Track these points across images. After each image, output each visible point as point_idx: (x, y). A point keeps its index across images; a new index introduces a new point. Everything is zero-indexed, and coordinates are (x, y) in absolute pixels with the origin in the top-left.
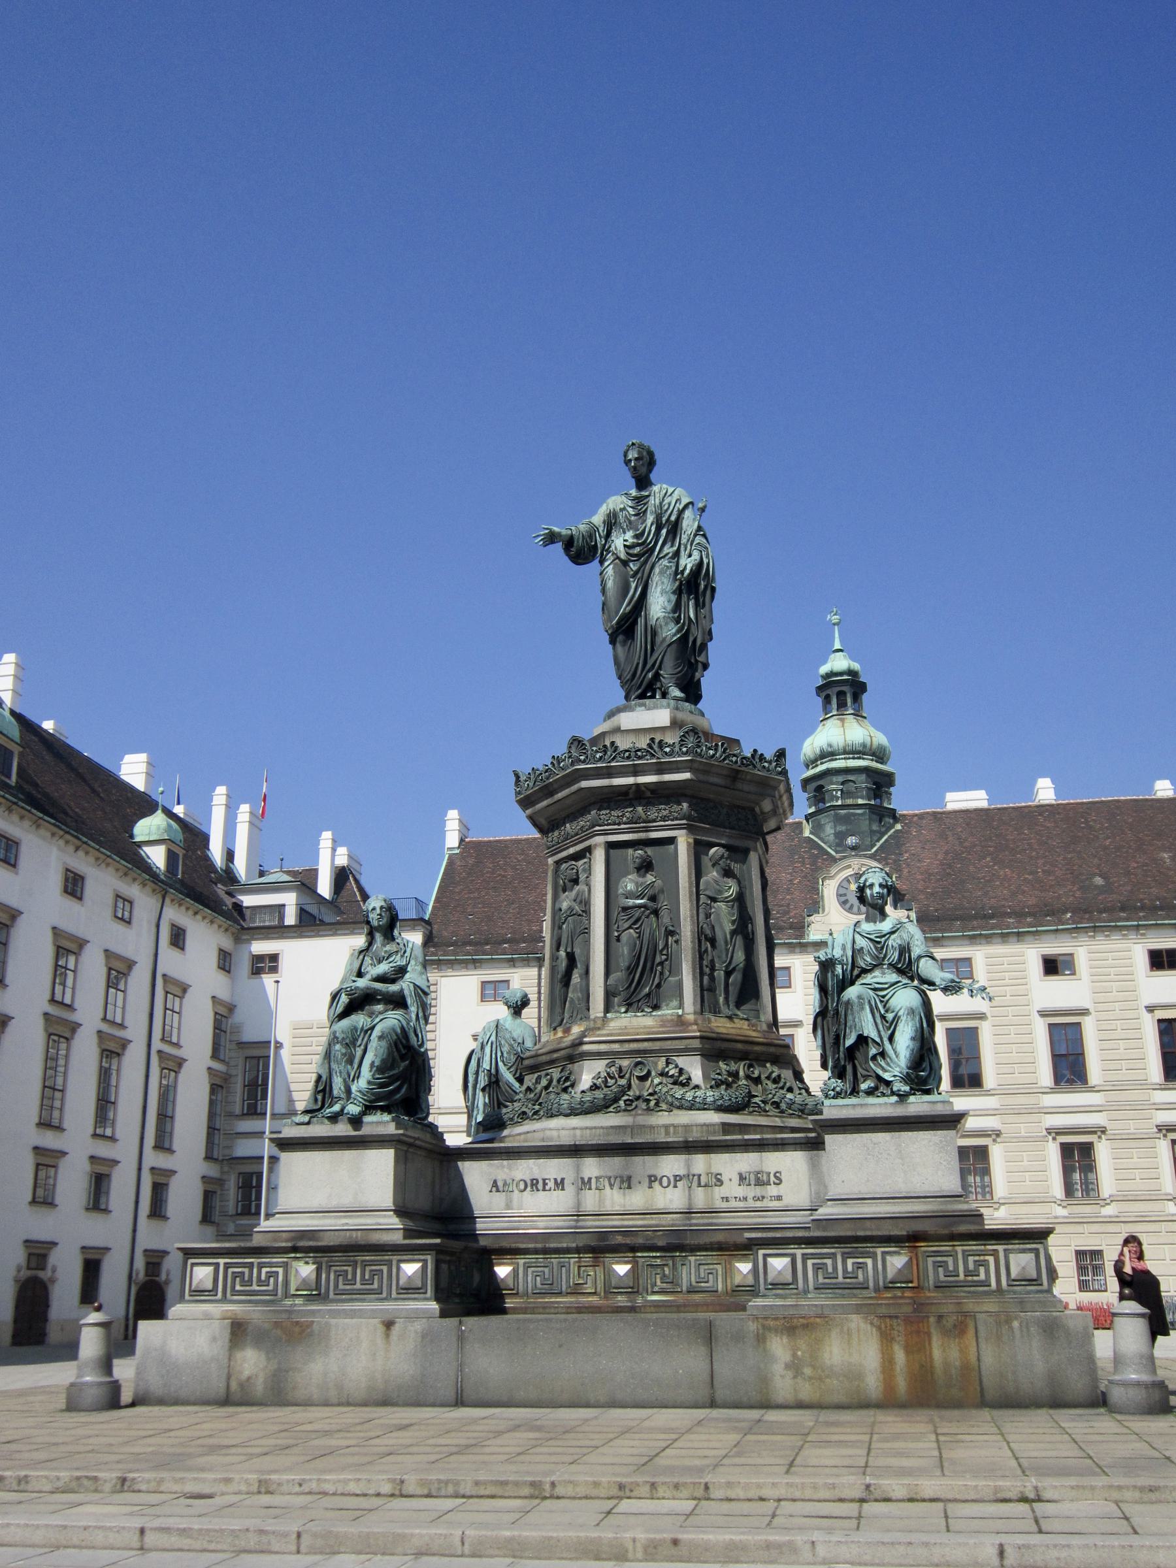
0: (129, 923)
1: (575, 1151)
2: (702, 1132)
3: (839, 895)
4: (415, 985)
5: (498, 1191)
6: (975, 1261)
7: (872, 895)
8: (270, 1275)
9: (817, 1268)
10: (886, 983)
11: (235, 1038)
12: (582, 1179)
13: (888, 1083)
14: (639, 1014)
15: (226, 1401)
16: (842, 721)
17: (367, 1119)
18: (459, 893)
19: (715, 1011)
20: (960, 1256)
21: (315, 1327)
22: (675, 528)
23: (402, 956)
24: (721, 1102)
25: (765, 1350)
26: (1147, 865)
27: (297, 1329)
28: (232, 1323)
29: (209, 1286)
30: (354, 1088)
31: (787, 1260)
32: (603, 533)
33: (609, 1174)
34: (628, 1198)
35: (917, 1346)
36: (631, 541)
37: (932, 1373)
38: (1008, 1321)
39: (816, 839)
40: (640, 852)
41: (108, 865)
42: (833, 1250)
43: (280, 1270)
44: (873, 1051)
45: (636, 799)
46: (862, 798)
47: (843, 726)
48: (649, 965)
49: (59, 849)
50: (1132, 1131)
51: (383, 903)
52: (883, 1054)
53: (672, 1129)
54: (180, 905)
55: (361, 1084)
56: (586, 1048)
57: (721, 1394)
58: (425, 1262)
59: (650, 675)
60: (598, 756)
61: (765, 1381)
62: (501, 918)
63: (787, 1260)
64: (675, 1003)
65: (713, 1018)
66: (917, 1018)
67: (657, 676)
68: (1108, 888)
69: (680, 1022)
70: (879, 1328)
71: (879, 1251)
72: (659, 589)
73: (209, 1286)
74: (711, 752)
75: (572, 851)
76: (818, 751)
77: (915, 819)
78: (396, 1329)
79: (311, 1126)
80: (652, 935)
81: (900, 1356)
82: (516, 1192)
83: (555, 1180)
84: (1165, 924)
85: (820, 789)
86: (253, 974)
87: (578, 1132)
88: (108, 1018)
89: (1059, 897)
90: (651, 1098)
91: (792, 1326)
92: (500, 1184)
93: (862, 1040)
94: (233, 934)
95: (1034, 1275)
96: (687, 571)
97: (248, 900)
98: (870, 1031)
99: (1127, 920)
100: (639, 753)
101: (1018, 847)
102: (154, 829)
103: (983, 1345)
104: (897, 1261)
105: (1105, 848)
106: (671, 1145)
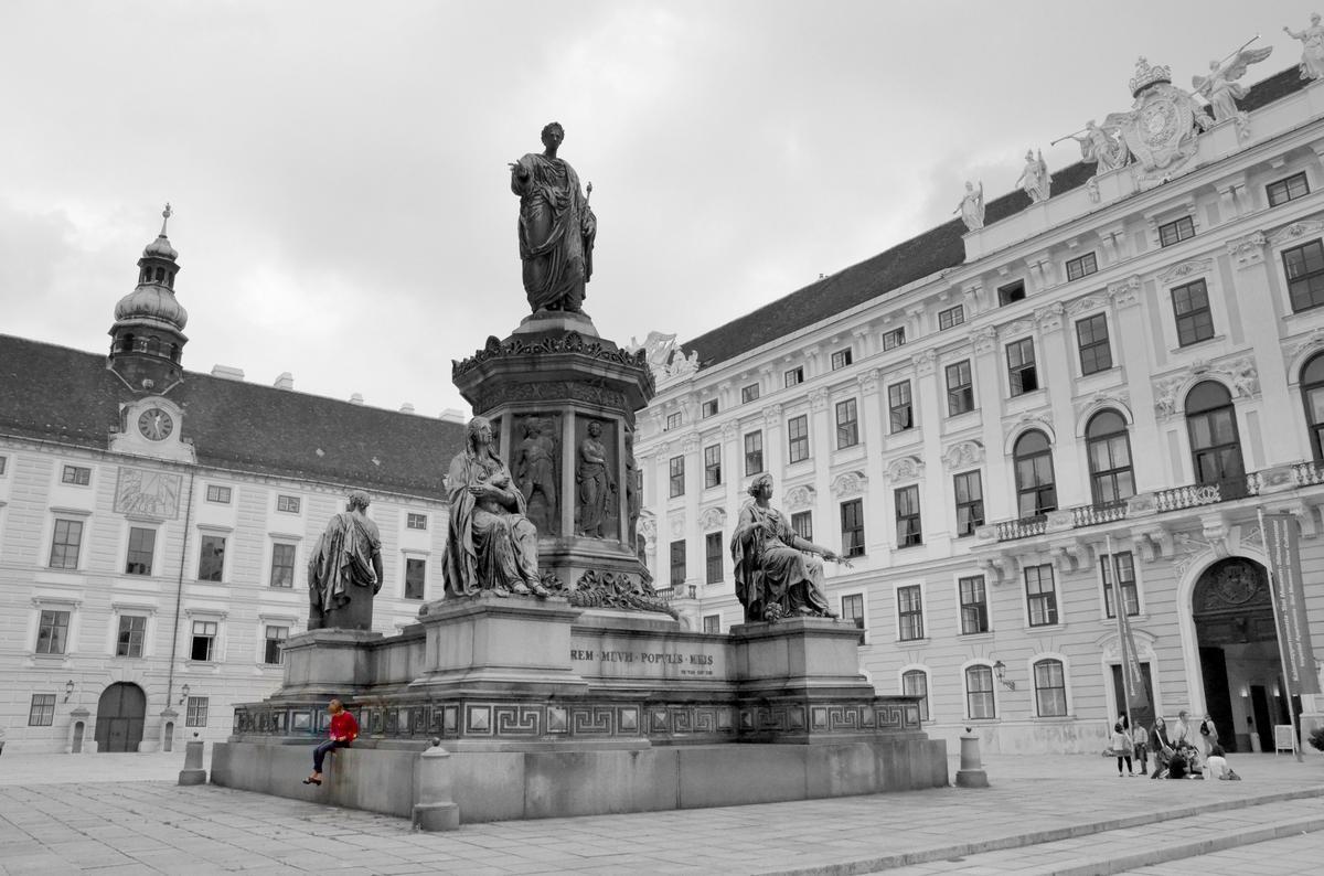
1: (602, 633)
3: (140, 422)
13: (820, 610)
15: (524, 817)
16: (158, 290)
21: (586, 757)
27: (573, 759)
29: (487, 726)
35: (888, 761)
43: (538, 713)
44: (811, 590)
52: (815, 591)
55: (532, 570)
56: (572, 558)
59: (562, 294)
61: (828, 781)
64: (614, 535)
75: (536, 409)
76: (135, 308)
87: (599, 620)
89: (296, 457)
93: (805, 582)
99: (338, 482)
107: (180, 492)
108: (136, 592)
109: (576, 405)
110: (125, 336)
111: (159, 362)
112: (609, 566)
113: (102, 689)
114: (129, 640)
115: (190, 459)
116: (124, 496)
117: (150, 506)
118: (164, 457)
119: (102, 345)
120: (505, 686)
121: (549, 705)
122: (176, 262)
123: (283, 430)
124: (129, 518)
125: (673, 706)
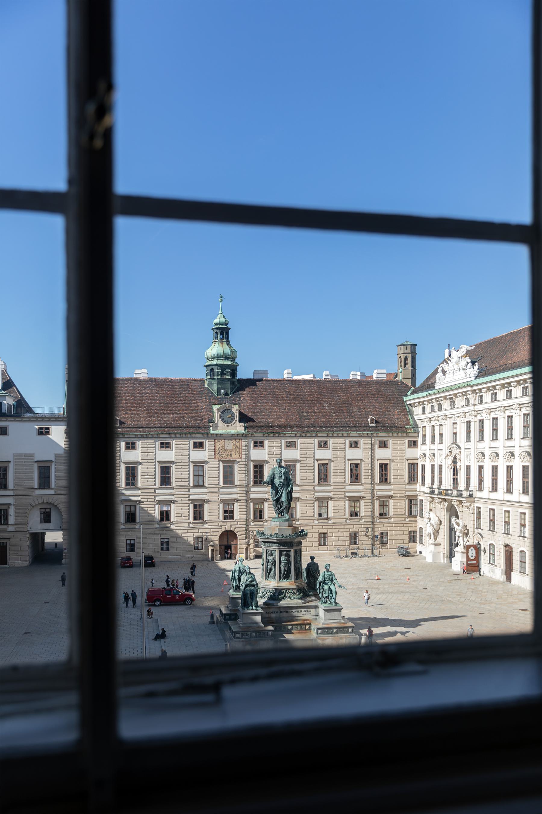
16: (222, 344)
26: (320, 408)
39: (210, 389)
44: (330, 598)
46: (228, 376)
47: (222, 347)
50: (307, 498)
67: (283, 511)
68: (308, 417)
76: (213, 356)
77: (244, 382)
84: (324, 433)
85: (212, 370)
98: (330, 595)
99: (313, 431)
101: (279, 398)
105: (307, 401)
107: (241, 446)
108: (228, 493)
110: (211, 370)
111: (226, 380)
113: (219, 534)
114: (229, 515)
115: (243, 431)
116: (218, 451)
117: (229, 454)
118: (233, 431)
119: (202, 374)
122: (229, 326)
123: (287, 404)
124: (222, 461)
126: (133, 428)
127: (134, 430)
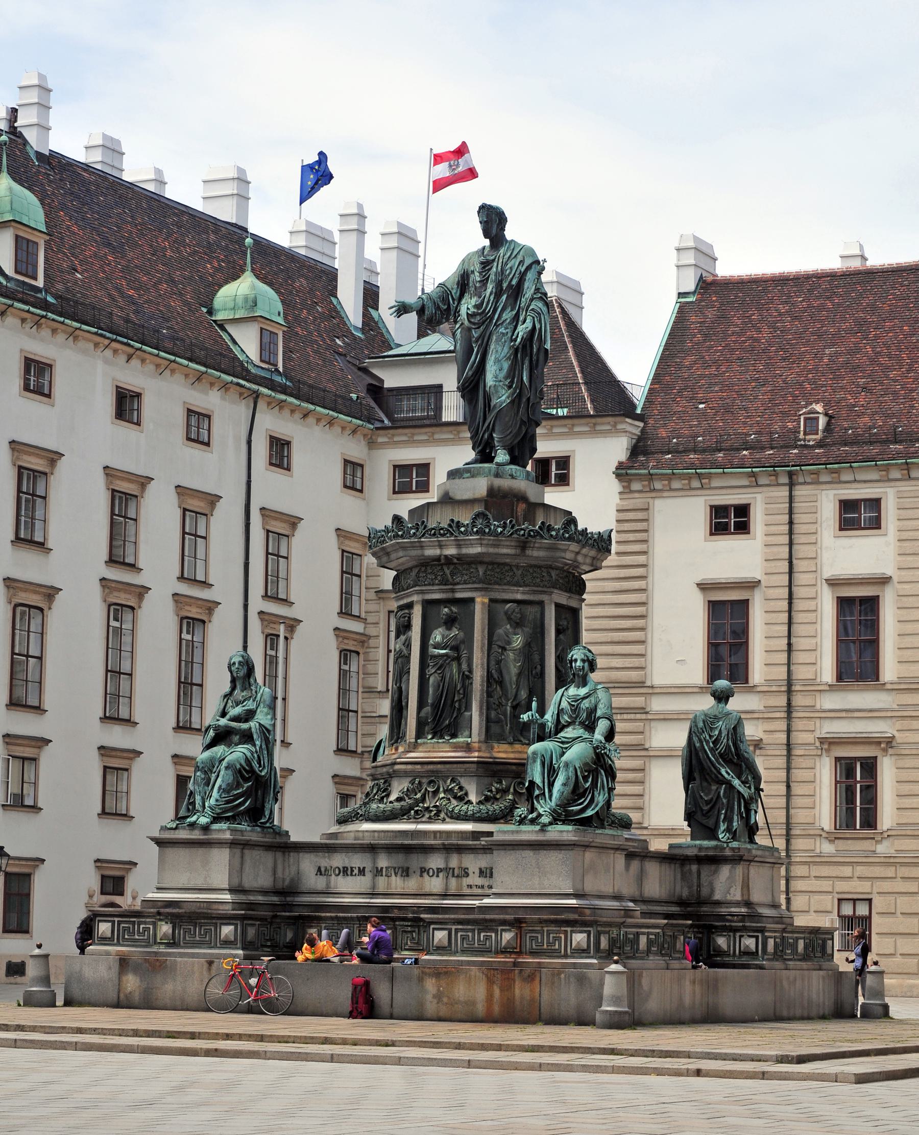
0: (208, 444)
1: (372, 849)
2: (458, 837)
4: (260, 724)
5: (321, 874)
6: (553, 937)
7: (575, 667)
8: (145, 929)
9: (463, 939)
10: (570, 738)
11: (372, 584)
12: (377, 868)
14: (440, 741)
15: (118, 1005)
17: (215, 826)
18: (690, 368)
19: (501, 738)
20: (545, 934)
22: (517, 291)
23: (254, 701)
24: (478, 815)
25: (423, 986)
27: (158, 964)
28: (120, 959)
29: (109, 935)
30: (207, 804)
31: (445, 933)
32: (456, 296)
33: (395, 865)
34: (406, 883)
35: (507, 988)
36: (472, 310)
37: (514, 1003)
38: (559, 974)
40: (446, 610)
41: (173, 371)
42: (473, 927)
43: (151, 927)
45: (446, 564)
48: (449, 702)
49: (106, 361)
51: (241, 659)
52: (544, 793)
53: (438, 834)
54: (281, 408)
56: (397, 767)
57: (396, 1011)
58: (236, 925)
59: (486, 436)
60: (412, 531)
61: (421, 1004)
62: (746, 409)
63: (445, 933)
64: (467, 733)
65: (496, 745)
66: (571, 769)
67: (491, 437)
69: (468, 748)
70: (487, 976)
71: (500, 928)
72: (493, 358)
73: (109, 935)
74: (499, 530)
78: (214, 966)
79: (177, 831)
80: (451, 677)
81: (497, 992)
82: (333, 876)
83: (359, 868)
86: (394, 492)
87: (376, 834)
88: (186, 575)
90: (434, 809)
91: (440, 972)
92: (323, 870)
93: (532, 783)
94: (365, 436)
95: (585, 946)
96: (519, 340)
97: (392, 379)
100: (442, 532)
102: (240, 301)
103: (543, 988)
104: (507, 936)
106: (435, 847)
109: (422, 592)
112: (433, 772)
120: (159, 903)
121: (160, 920)
125: (402, 923)
126: (871, 443)
127: (875, 450)
